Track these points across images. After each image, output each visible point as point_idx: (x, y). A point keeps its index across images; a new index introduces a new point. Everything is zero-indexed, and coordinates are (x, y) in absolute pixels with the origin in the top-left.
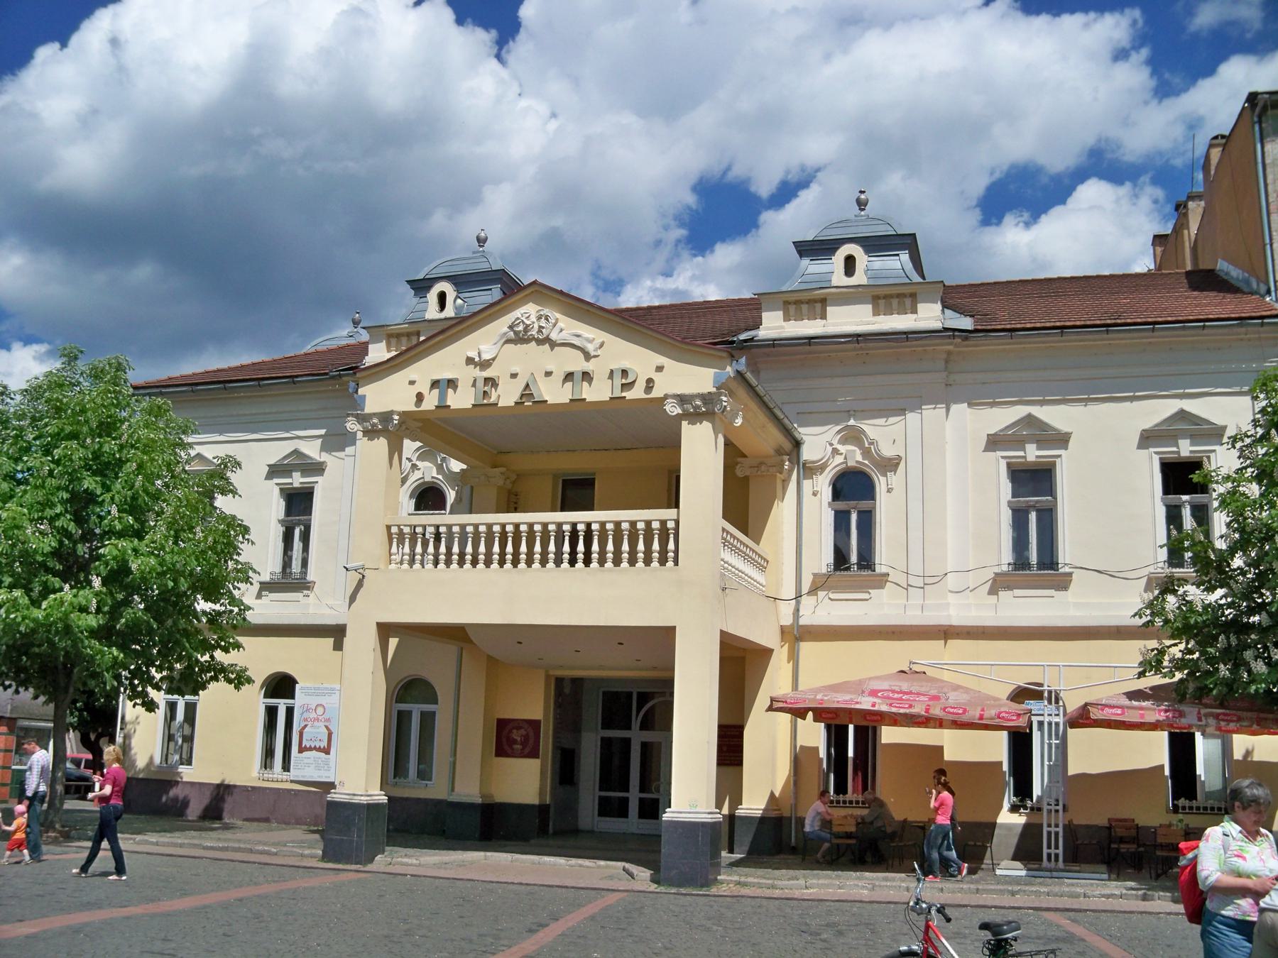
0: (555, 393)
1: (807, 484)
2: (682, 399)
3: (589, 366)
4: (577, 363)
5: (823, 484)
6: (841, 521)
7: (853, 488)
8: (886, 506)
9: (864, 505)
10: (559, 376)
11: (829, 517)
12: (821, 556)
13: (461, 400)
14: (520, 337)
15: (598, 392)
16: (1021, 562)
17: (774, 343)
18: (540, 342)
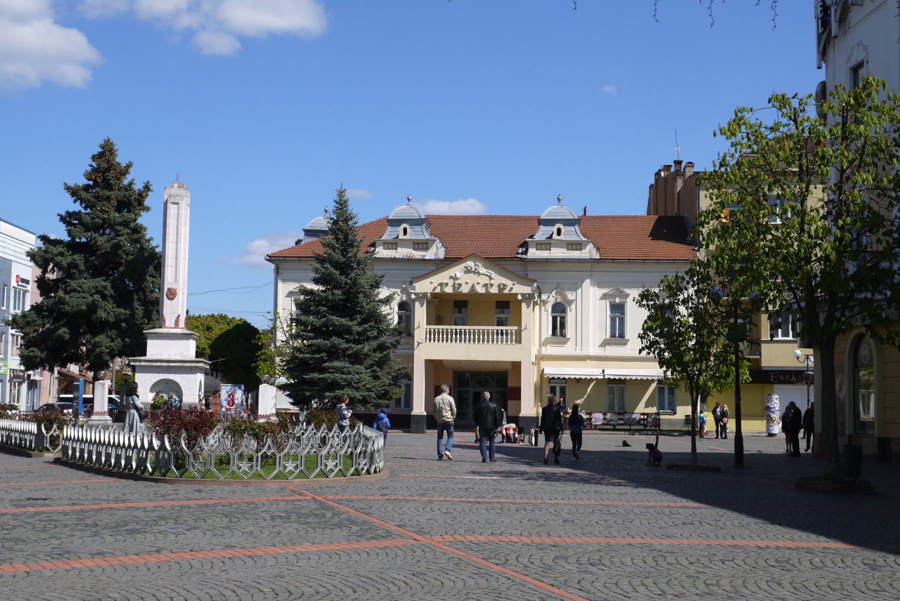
0: (480, 290)
1: (543, 308)
2: (522, 295)
3: (492, 282)
4: (486, 280)
5: (549, 307)
6: (554, 319)
7: (559, 309)
8: (570, 317)
9: (562, 315)
10: (482, 285)
11: (550, 319)
12: (548, 331)
13: (449, 290)
14: (468, 271)
15: (494, 290)
16: (613, 335)
17: (535, 261)
18: (475, 273)
